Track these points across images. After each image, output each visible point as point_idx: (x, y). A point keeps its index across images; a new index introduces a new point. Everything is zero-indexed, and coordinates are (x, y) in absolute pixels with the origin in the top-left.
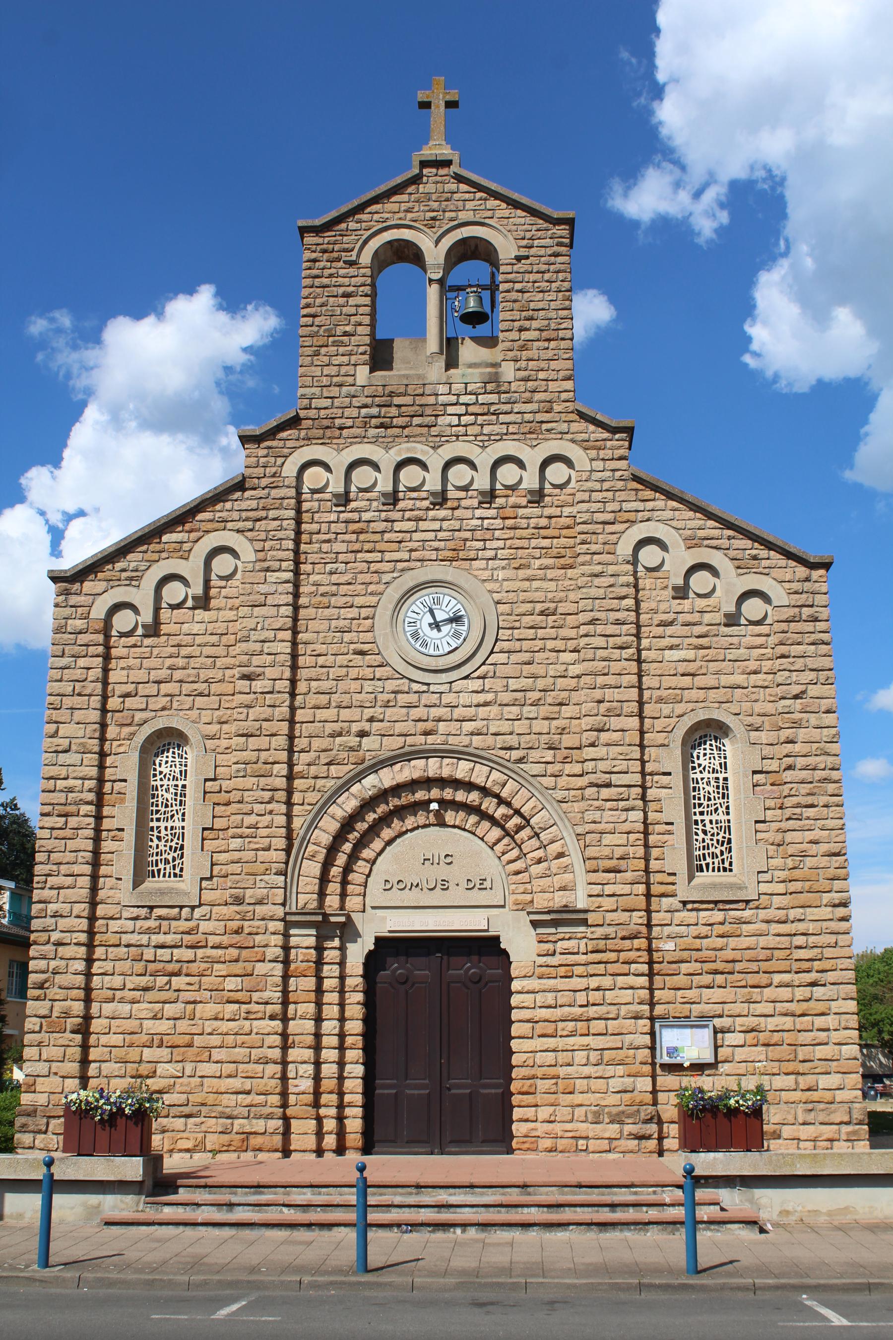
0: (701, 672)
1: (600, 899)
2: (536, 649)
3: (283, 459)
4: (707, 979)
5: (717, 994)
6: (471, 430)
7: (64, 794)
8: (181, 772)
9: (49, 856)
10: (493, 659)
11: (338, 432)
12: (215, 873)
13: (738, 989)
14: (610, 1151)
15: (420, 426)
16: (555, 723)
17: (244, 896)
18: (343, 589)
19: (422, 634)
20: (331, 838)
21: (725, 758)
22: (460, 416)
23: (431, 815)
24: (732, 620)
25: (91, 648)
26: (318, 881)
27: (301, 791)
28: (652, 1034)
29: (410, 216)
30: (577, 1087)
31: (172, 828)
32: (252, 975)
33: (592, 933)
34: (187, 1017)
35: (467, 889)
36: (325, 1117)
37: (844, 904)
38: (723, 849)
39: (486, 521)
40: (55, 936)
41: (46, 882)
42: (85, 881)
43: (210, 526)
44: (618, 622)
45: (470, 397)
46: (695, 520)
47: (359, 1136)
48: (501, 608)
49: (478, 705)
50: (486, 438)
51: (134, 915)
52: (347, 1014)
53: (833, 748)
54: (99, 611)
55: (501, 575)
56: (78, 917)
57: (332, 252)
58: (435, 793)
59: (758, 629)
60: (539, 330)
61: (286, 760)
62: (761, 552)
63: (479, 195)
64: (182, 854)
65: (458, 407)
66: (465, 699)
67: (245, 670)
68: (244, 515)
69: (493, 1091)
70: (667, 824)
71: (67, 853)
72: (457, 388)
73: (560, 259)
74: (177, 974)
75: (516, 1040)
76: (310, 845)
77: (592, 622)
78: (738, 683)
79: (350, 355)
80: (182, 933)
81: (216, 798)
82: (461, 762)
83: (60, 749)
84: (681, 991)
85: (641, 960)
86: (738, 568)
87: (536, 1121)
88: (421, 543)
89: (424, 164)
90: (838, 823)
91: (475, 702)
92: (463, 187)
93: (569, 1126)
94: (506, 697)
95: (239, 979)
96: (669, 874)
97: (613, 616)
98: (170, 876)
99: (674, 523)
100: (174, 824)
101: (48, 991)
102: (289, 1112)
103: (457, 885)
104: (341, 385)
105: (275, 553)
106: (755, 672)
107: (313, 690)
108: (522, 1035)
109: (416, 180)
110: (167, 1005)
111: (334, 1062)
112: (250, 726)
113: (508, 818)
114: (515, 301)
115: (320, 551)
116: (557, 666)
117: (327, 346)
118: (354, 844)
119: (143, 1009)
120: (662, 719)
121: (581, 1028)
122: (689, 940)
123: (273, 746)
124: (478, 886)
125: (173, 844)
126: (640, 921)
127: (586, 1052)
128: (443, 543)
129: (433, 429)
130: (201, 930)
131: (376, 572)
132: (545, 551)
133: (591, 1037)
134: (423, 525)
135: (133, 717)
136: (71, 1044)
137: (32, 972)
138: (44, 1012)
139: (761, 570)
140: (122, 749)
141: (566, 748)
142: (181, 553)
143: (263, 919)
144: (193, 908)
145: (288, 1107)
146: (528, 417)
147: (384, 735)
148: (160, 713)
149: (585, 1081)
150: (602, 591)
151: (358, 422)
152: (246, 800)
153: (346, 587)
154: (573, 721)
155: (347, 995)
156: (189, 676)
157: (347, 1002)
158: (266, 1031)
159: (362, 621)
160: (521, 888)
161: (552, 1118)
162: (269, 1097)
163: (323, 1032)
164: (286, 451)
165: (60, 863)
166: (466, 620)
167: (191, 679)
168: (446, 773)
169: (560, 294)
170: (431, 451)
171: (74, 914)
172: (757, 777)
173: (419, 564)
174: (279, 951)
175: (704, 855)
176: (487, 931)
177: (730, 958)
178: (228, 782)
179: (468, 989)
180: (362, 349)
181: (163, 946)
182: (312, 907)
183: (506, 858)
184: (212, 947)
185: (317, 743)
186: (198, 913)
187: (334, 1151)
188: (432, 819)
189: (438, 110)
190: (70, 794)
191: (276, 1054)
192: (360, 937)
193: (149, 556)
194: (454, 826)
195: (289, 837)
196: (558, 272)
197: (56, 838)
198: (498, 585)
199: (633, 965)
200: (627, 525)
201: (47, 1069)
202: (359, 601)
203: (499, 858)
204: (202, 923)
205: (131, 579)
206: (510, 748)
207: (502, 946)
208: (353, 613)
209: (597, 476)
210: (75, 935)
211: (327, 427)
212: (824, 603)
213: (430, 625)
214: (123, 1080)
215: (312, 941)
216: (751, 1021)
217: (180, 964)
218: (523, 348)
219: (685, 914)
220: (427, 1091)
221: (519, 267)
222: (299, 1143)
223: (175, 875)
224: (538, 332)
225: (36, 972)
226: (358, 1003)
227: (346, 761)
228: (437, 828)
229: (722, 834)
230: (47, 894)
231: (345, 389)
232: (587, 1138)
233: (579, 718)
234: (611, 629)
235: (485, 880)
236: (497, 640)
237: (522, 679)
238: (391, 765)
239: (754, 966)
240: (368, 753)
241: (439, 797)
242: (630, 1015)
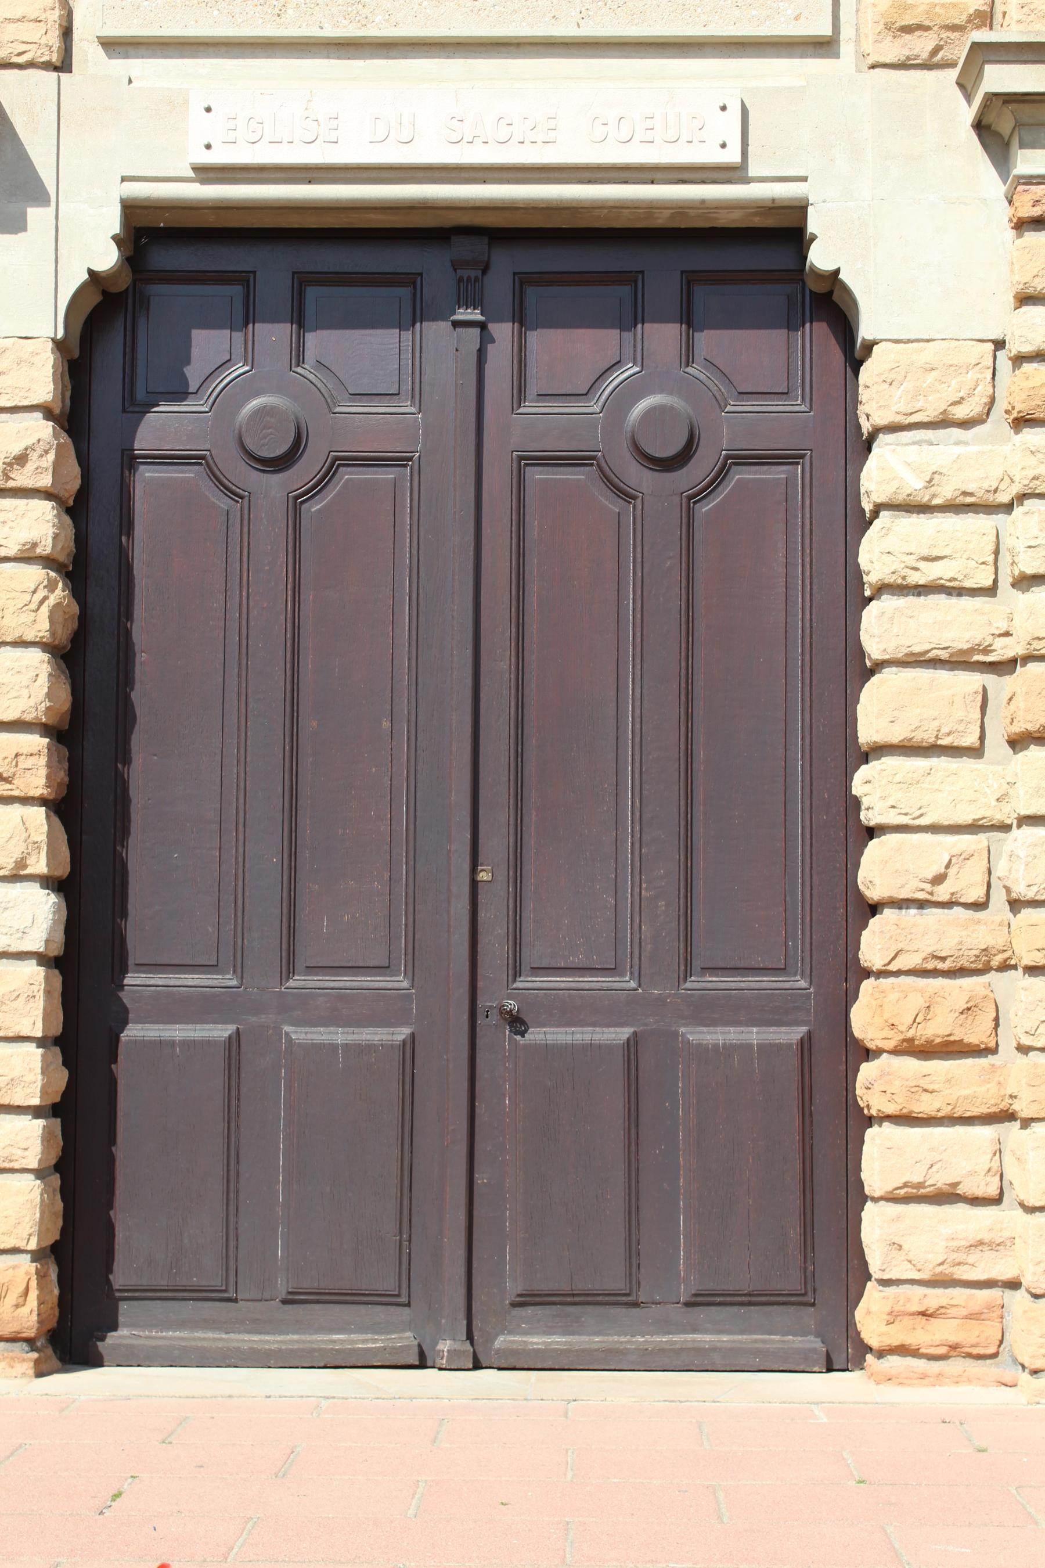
47: (25, 1267)
69: (754, 1035)
75: (888, 763)
87: (997, 1201)
108: (926, 736)
179: (626, 495)
192: (39, 196)
220: (402, 1033)
226: (26, 557)
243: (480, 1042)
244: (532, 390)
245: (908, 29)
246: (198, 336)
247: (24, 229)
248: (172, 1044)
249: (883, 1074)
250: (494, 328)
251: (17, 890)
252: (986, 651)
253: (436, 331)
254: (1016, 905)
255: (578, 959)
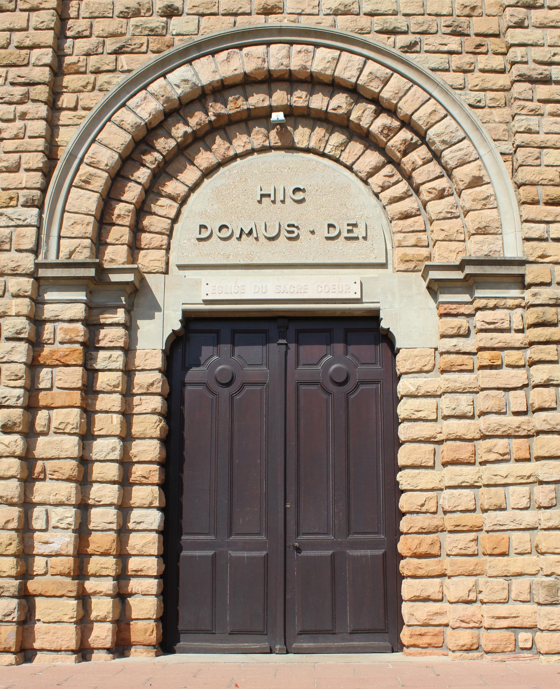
1: (544, 244)
20: (117, 156)
23: (273, 134)
26: (92, 219)
27: (74, 92)
30: (514, 544)
33: (535, 295)
35: (328, 238)
36: (95, 593)
47: (152, 624)
52: (136, 430)
69: (369, 552)
75: (407, 471)
76: (83, 166)
93: (502, 610)
102: (33, 586)
103: (313, 232)
108: (418, 463)
111: (111, 505)
113: (390, 132)
118: (153, 170)
121: (519, 449)
123: (32, 24)
127: (526, 488)
141: (477, 35)
145: (32, 577)
147: (203, 15)
149: (527, 534)
155: (136, 400)
157: (136, 410)
160: (412, 239)
161: (472, 597)
163: (94, 457)
174: (22, 323)
179: (329, 393)
183: (386, 195)
185: (100, 26)
187: (109, 650)
188: (274, 138)
192: (159, 309)
194: (307, 150)
203: (377, 195)
215: (79, 311)
220: (264, 553)
222: (48, 637)
226: (153, 413)
227: (144, 49)
228: (282, 153)
232: (532, 628)
235: (355, 225)
238: (213, 54)
241: (285, 102)
243: (288, 556)
244: (301, 363)
245: (407, 261)
246: (204, 348)
247: (154, 318)
248: (195, 557)
249: (407, 563)
250: (290, 345)
251: (150, 511)
252: (435, 438)
253: (273, 346)
254: (445, 512)
255: (317, 530)
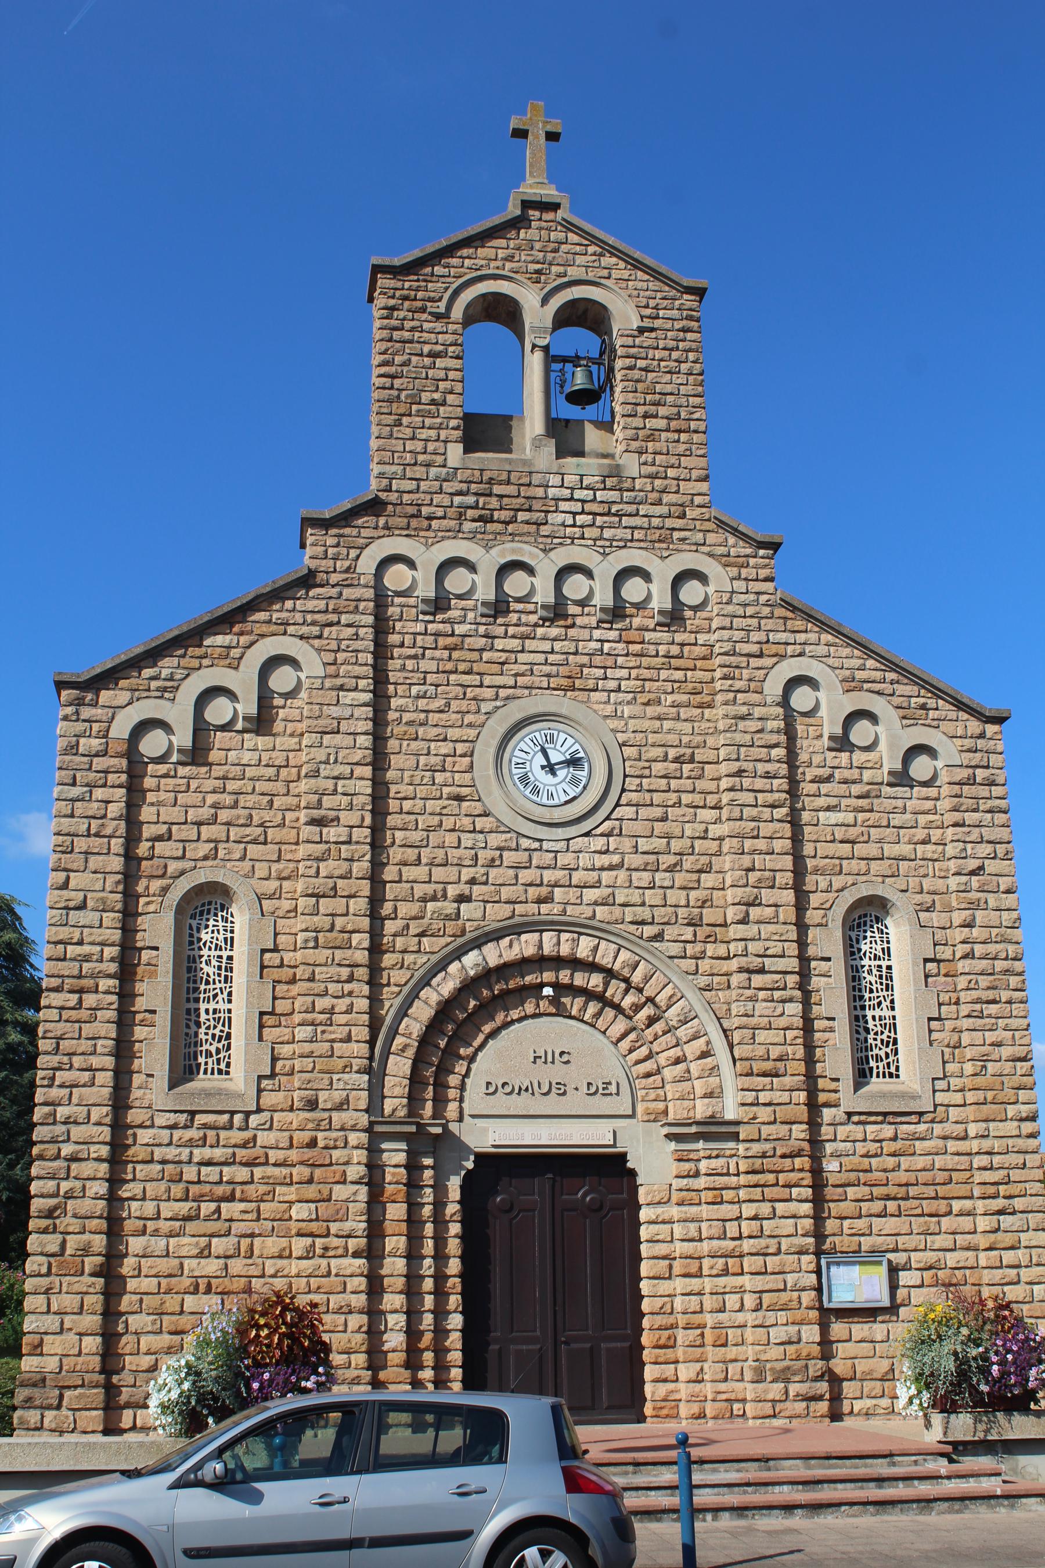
0: (862, 839)
1: (755, 1108)
2: (670, 803)
3: (358, 551)
4: (877, 1206)
5: (890, 1224)
6: (589, 533)
7: (77, 964)
8: (226, 939)
9: (58, 1044)
10: (619, 812)
11: (426, 523)
12: (277, 1070)
13: (913, 1219)
14: (774, 1416)
15: (527, 523)
16: (693, 894)
17: (317, 1100)
18: (433, 718)
19: (532, 779)
21: (888, 942)
22: (575, 514)
24: (902, 778)
25: (110, 776)
28: (818, 1272)
29: (509, 265)
31: (215, 1011)
32: (329, 1200)
34: (243, 1254)
37: (1033, 1118)
38: (889, 1050)
39: (606, 646)
40: (67, 1150)
41: (53, 1078)
42: (106, 1078)
43: (265, 629)
44: (767, 776)
45: (586, 492)
46: (850, 658)
48: (628, 751)
49: (602, 869)
50: (608, 544)
51: (171, 1122)
53: (1017, 934)
54: (121, 729)
55: (627, 710)
56: (98, 1124)
57: (415, 299)
58: (548, 976)
59: (925, 791)
60: (667, 418)
61: (367, 928)
62: (929, 701)
63: (591, 249)
64: (229, 1045)
65: (572, 503)
66: (584, 860)
67: (316, 813)
68: (309, 618)
69: (619, 1345)
70: (829, 1019)
71: (83, 1041)
72: (570, 480)
73: (689, 336)
74: (231, 1198)
77: (739, 773)
78: (904, 853)
79: (439, 428)
80: (235, 1146)
81: (276, 974)
82: (582, 938)
83: (72, 904)
84: (848, 1221)
85: (805, 1183)
86: (904, 718)
88: (528, 667)
89: (526, 205)
90: (1024, 1022)
91: (598, 865)
92: (573, 237)
94: (637, 860)
95: (313, 1206)
96: (833, 1080)
97: (761, 768)
98: (212, 1073)
99: (830, 661)
100: (217, 1007)
101: (58, 1221)
104: (428, 465)
105: (350, 667)
106: (924, 842)
107: (398, 842)
109: (519, 223)
110: (215, 1240)
112: (321, 884)
114: (638, 381)
115: (403, 668)
116: (696, 825)
117: (410, 415)
119: (186, 1244)
120: (819, 894)
122: (856, 1159)
123: (351, 911)
124: (601, 1091)
125: (217, 1032)
126: (802, 1136)
127: (738, 1296)
128: (555, 668)
129: (542, 528)
130: (259, 1143)
131: (474, 699)
132: (676, 685)
133: (747, 1277)
134: (530, 644)
135: (166, 866)
136: (91, 1290)
137: (36, 1196)
138: (54, 1248)
139: (927, 722)
140: (152, 908)
142: (228, 661)
143: (342, 1129)
144: (248, 1114)
146: (656, 522)
148: (199, 864)
150: (748, 737)
151: (451, 512)
152: (317, 977)
153: (437, 715)
154: (715, 892)
156: (238, 817)
158: (348, 1272)
159: (458, 759)
160: (652, 1095)
162: (353, 1356)
164: (361, 541)
165: (74, 1054)
166: (586, 765)
167: (242, 821)
168: (565, 950)
169: (691, 378)
170: (542, 555)
171: (93, 1119)
172: (929, 965)
173: (526, 692)
175: (867, 1057)
176: (614, 1146)
177: (904, 1181)
178: (291, 954)
180: (453, 423)
181: (209, 1163)
182: (402, 1114)
184: (275, 1165)
186: (254, 1121)
189: (537, 141)
190: (85, 965)
191: (360, 1300)
193: (184, 662)
195: (374, 1026)
196: (690, 350)
197: (67, 1021)
198: (623, 723)
199: (794, 1190)
200: (775, 660)
201: (58, 1324)
202: (453, 733)
204: (259, 1133)
205: (165, 689)
206: (643, 923)
207: (629, 1165)
208: (445, 748)
209: (738, 598)
210: (93, 1148)
211: (413, 516)
212: (1000, 765)
213: (543, 767)
214: (158, 1337)
216: (930, 1257)
217: (231, 1187)
218: (651, 438)
219: (851, 1127)
221: (646, 339)
223: (220, 1072)
224: (665, 421)
225: (42, 1196)
229: (886, 1033)
230: (55, 1093)
231: (433, 471)
233: (723, 889)
234: (760, 783)
235: (610, 1083)
236: (623, 790)
237: (653, 839)
239: (930, 1191)
240: (468, 924)
242: (793, 1250)
